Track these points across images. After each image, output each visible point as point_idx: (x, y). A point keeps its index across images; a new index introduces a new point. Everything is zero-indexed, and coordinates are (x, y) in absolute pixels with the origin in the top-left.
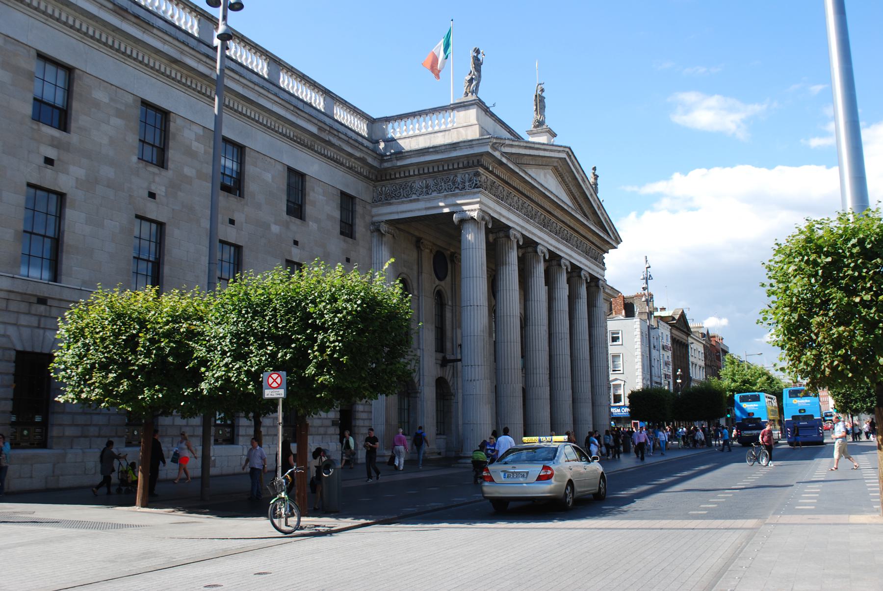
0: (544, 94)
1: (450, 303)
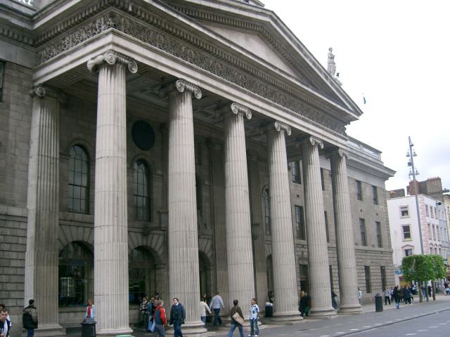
1: (159, 172)
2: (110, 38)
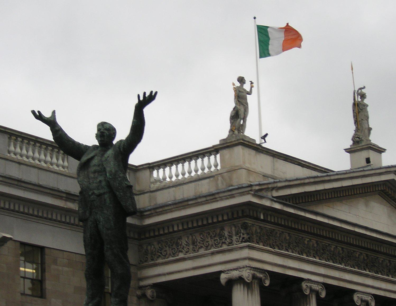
0: (366, 101)
2: (246, 253)
